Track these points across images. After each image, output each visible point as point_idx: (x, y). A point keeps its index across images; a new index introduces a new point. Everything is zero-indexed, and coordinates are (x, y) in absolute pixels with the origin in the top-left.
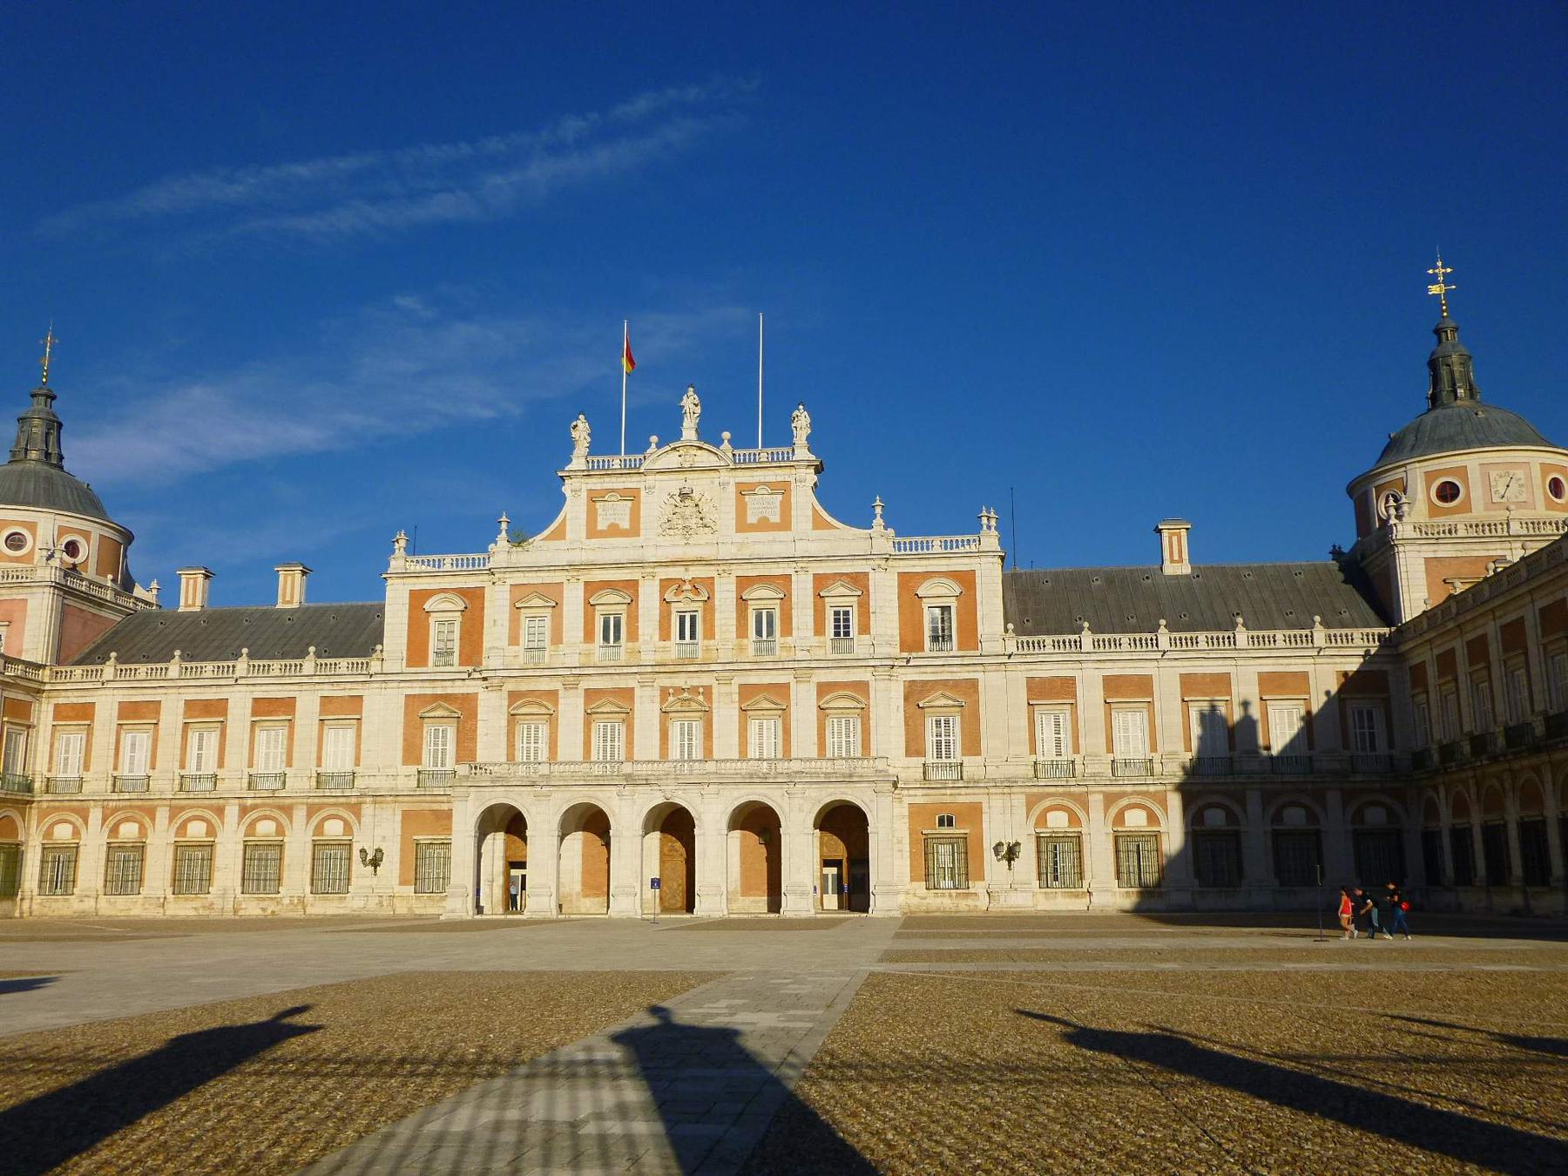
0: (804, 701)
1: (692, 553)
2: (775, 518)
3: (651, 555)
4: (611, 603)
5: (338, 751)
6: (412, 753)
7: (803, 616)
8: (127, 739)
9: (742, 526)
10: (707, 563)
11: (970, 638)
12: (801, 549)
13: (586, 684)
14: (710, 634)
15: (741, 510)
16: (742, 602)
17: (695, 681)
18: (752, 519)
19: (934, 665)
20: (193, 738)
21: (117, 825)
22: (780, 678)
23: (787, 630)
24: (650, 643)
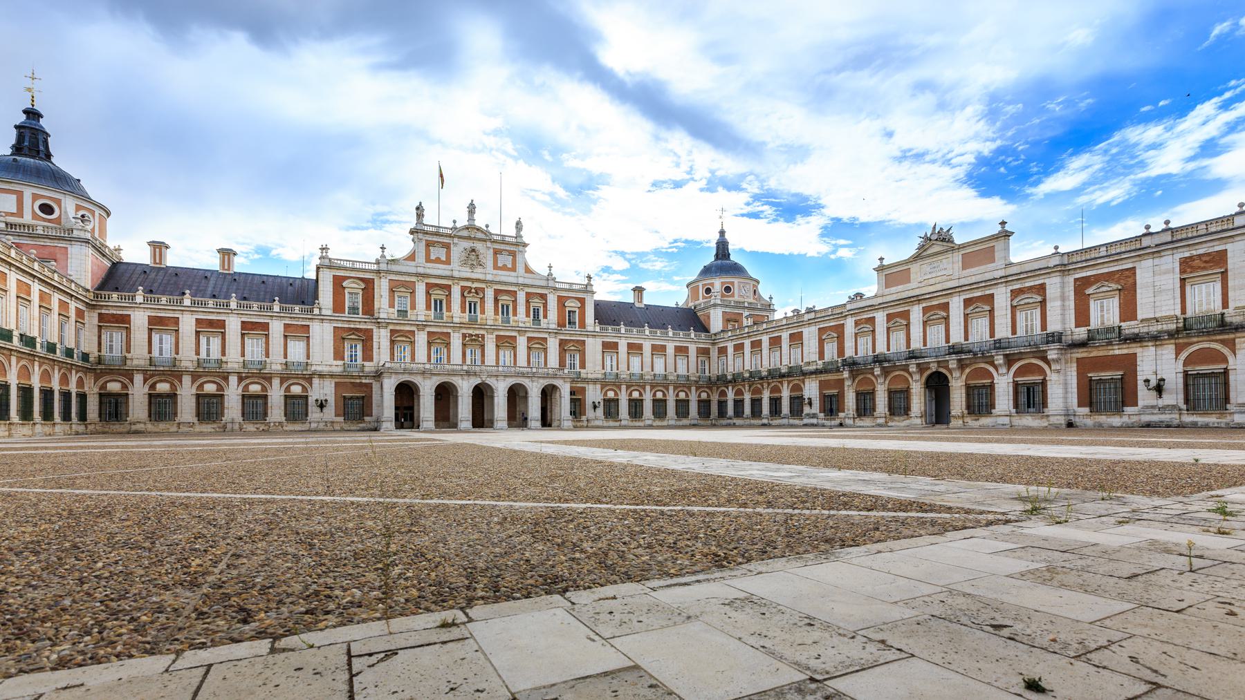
0: (522, 342)
2: (510, 266)
3: (456, 274)
4: (438, 294)
5: (296, 351)
7: (521, 309)
8: (156, 338)
9: (496, 267)
10: (478, 280)
11: (583, 324)
12: (521, 281)
13: (428, 329)
14: (483, 312)
16: (496, 300)
17: (477, 332)
18: (500, 265)
19: (570, 333)
20: (203, 340)
21: (155, 384)
22: (513, 334)
23: (515, 314)
24: (456, 312)
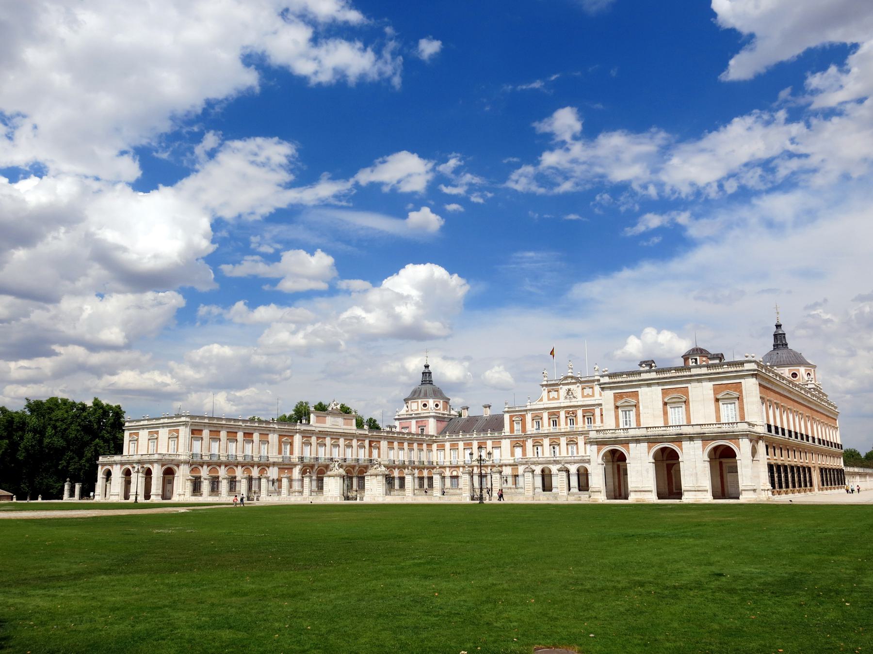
1: (572, 404)
3: (562, 405)
6: (513, 454)
9: (583, 396)
15: (583, 393)
